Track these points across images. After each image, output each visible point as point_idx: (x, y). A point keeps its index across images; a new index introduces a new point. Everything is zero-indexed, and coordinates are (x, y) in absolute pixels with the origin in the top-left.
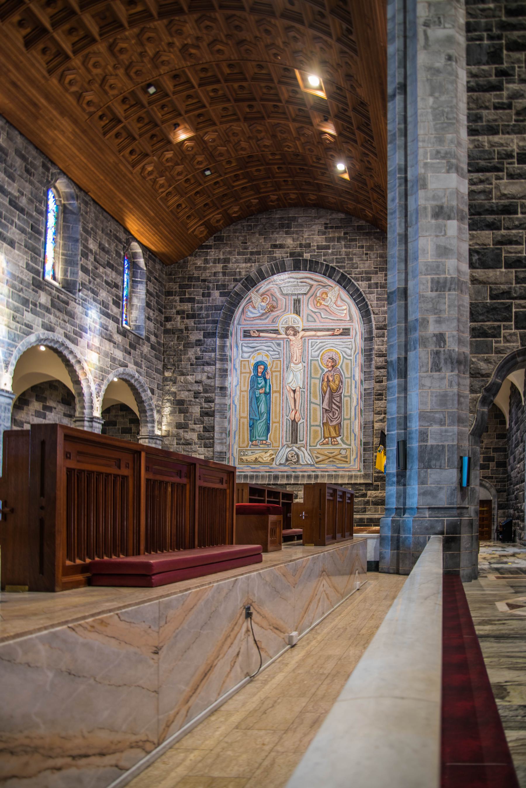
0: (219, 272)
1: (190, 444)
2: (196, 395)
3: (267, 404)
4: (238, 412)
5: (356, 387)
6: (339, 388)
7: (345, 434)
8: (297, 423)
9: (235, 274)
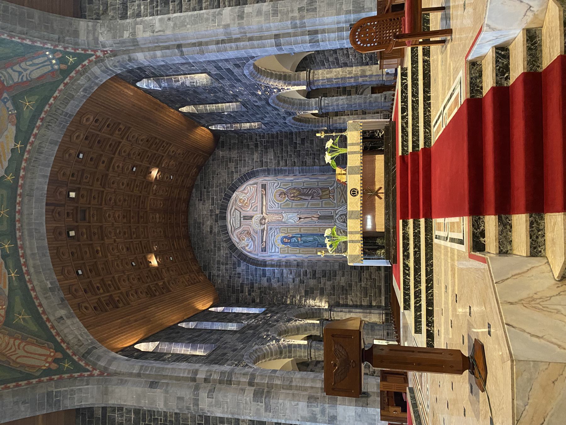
0: (225, 268)
1: (334, 286)
2: (302, 282)
3: (307, 236)
4: (313, 255)
5: (298, 179)
6: (298, 190)
7: (327, 184)
8: (320, 216)
9: (227, 257)
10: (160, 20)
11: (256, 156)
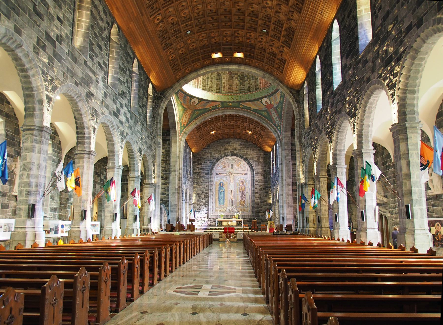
6: (244, 190)
10: (289, 159)
11: (260, 171)
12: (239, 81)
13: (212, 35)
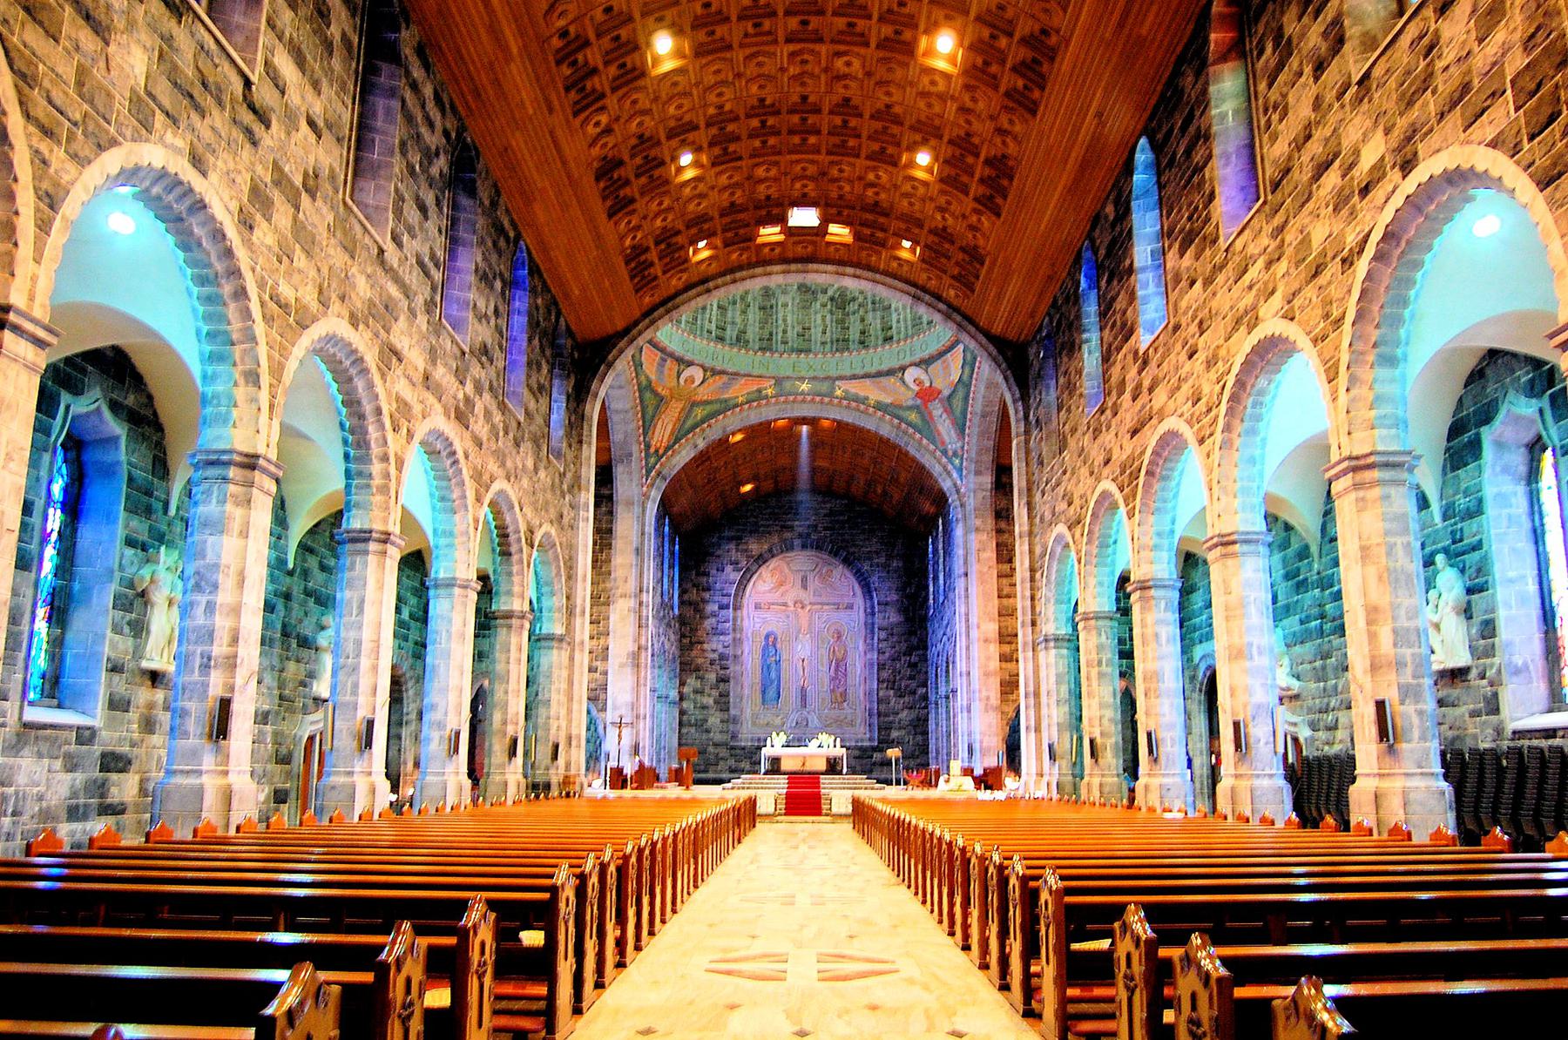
2: (712, 663)
6: (844, 658)
12: (831, 312)
13: (760, 172)
